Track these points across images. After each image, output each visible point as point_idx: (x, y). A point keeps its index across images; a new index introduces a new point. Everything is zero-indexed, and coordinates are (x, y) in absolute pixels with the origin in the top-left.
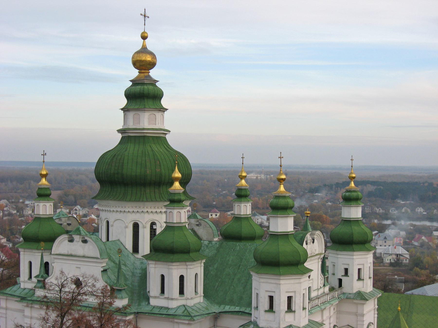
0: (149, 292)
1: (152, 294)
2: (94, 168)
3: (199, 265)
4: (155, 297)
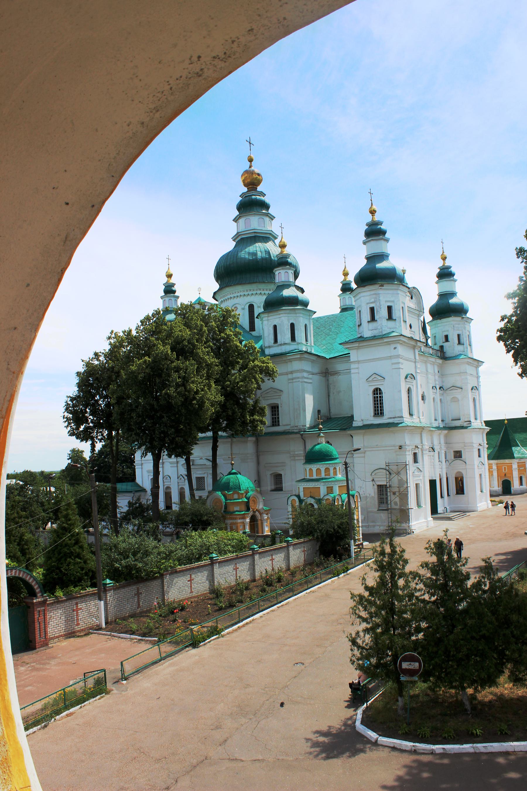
4: (269, 347)
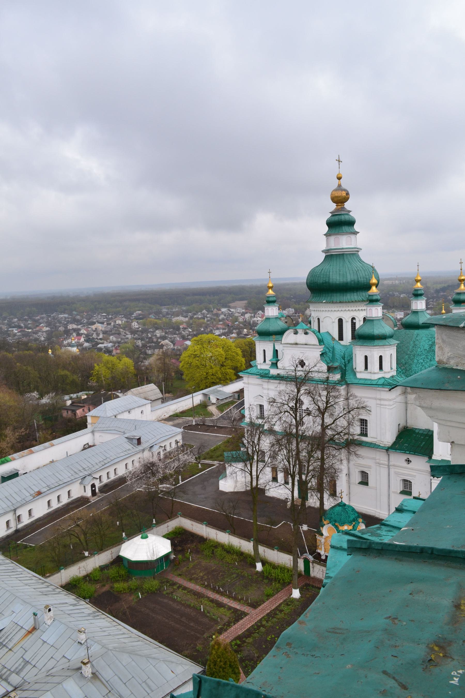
0: (355, 368)
1: (358, 370)
2: (305, 281)
3: (393, 348)
4: (361, 372)
